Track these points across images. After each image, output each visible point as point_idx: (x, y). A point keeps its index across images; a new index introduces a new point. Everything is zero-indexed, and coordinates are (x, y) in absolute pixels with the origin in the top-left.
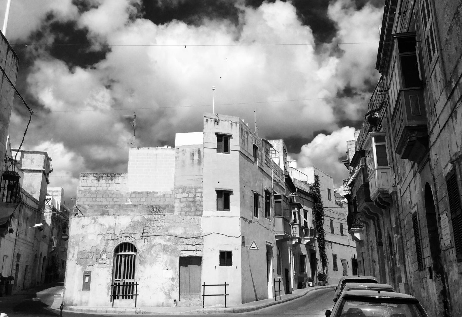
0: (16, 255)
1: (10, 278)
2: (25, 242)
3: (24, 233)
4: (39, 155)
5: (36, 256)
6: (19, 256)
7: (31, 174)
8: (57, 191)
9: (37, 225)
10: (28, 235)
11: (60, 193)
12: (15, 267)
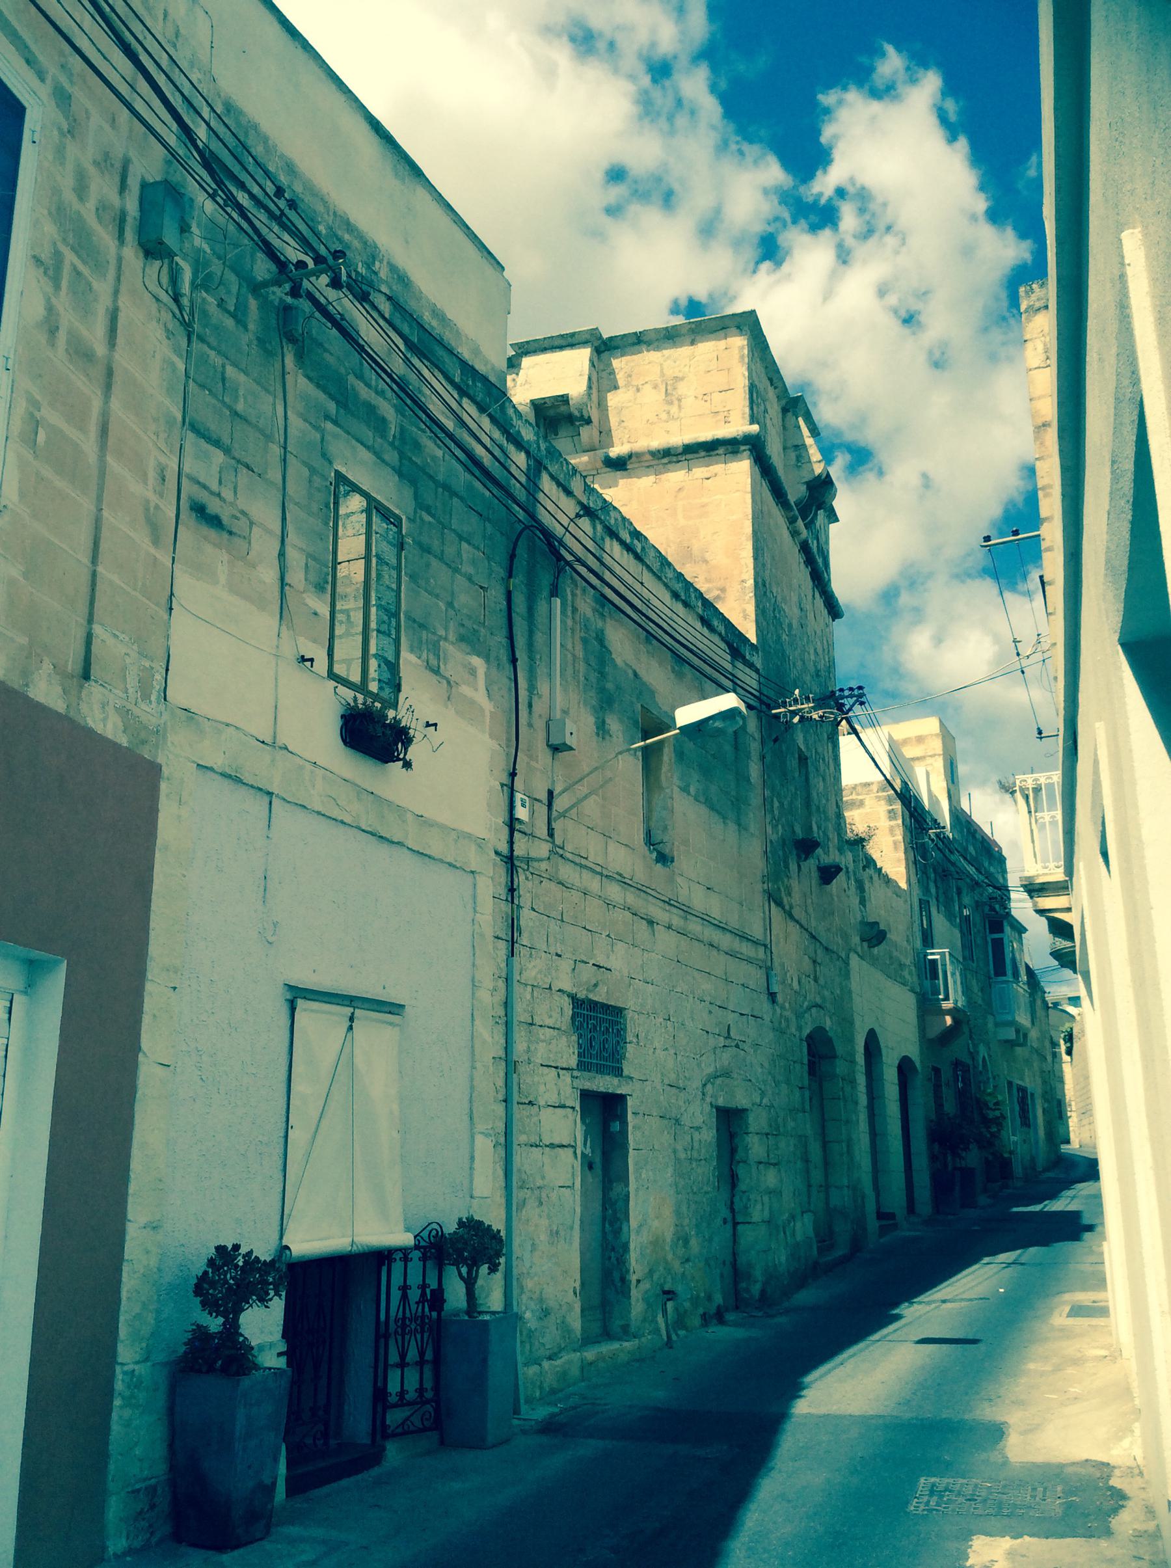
0: (558, 1012)
1: (470, 1246)
2: (657, 912)
4: (707, 349)
5: (819, 1052)
6: (599, 1028)
7: (676, 477)
8: (920, 739)
11: (937, 745)
12: (565, 1126)
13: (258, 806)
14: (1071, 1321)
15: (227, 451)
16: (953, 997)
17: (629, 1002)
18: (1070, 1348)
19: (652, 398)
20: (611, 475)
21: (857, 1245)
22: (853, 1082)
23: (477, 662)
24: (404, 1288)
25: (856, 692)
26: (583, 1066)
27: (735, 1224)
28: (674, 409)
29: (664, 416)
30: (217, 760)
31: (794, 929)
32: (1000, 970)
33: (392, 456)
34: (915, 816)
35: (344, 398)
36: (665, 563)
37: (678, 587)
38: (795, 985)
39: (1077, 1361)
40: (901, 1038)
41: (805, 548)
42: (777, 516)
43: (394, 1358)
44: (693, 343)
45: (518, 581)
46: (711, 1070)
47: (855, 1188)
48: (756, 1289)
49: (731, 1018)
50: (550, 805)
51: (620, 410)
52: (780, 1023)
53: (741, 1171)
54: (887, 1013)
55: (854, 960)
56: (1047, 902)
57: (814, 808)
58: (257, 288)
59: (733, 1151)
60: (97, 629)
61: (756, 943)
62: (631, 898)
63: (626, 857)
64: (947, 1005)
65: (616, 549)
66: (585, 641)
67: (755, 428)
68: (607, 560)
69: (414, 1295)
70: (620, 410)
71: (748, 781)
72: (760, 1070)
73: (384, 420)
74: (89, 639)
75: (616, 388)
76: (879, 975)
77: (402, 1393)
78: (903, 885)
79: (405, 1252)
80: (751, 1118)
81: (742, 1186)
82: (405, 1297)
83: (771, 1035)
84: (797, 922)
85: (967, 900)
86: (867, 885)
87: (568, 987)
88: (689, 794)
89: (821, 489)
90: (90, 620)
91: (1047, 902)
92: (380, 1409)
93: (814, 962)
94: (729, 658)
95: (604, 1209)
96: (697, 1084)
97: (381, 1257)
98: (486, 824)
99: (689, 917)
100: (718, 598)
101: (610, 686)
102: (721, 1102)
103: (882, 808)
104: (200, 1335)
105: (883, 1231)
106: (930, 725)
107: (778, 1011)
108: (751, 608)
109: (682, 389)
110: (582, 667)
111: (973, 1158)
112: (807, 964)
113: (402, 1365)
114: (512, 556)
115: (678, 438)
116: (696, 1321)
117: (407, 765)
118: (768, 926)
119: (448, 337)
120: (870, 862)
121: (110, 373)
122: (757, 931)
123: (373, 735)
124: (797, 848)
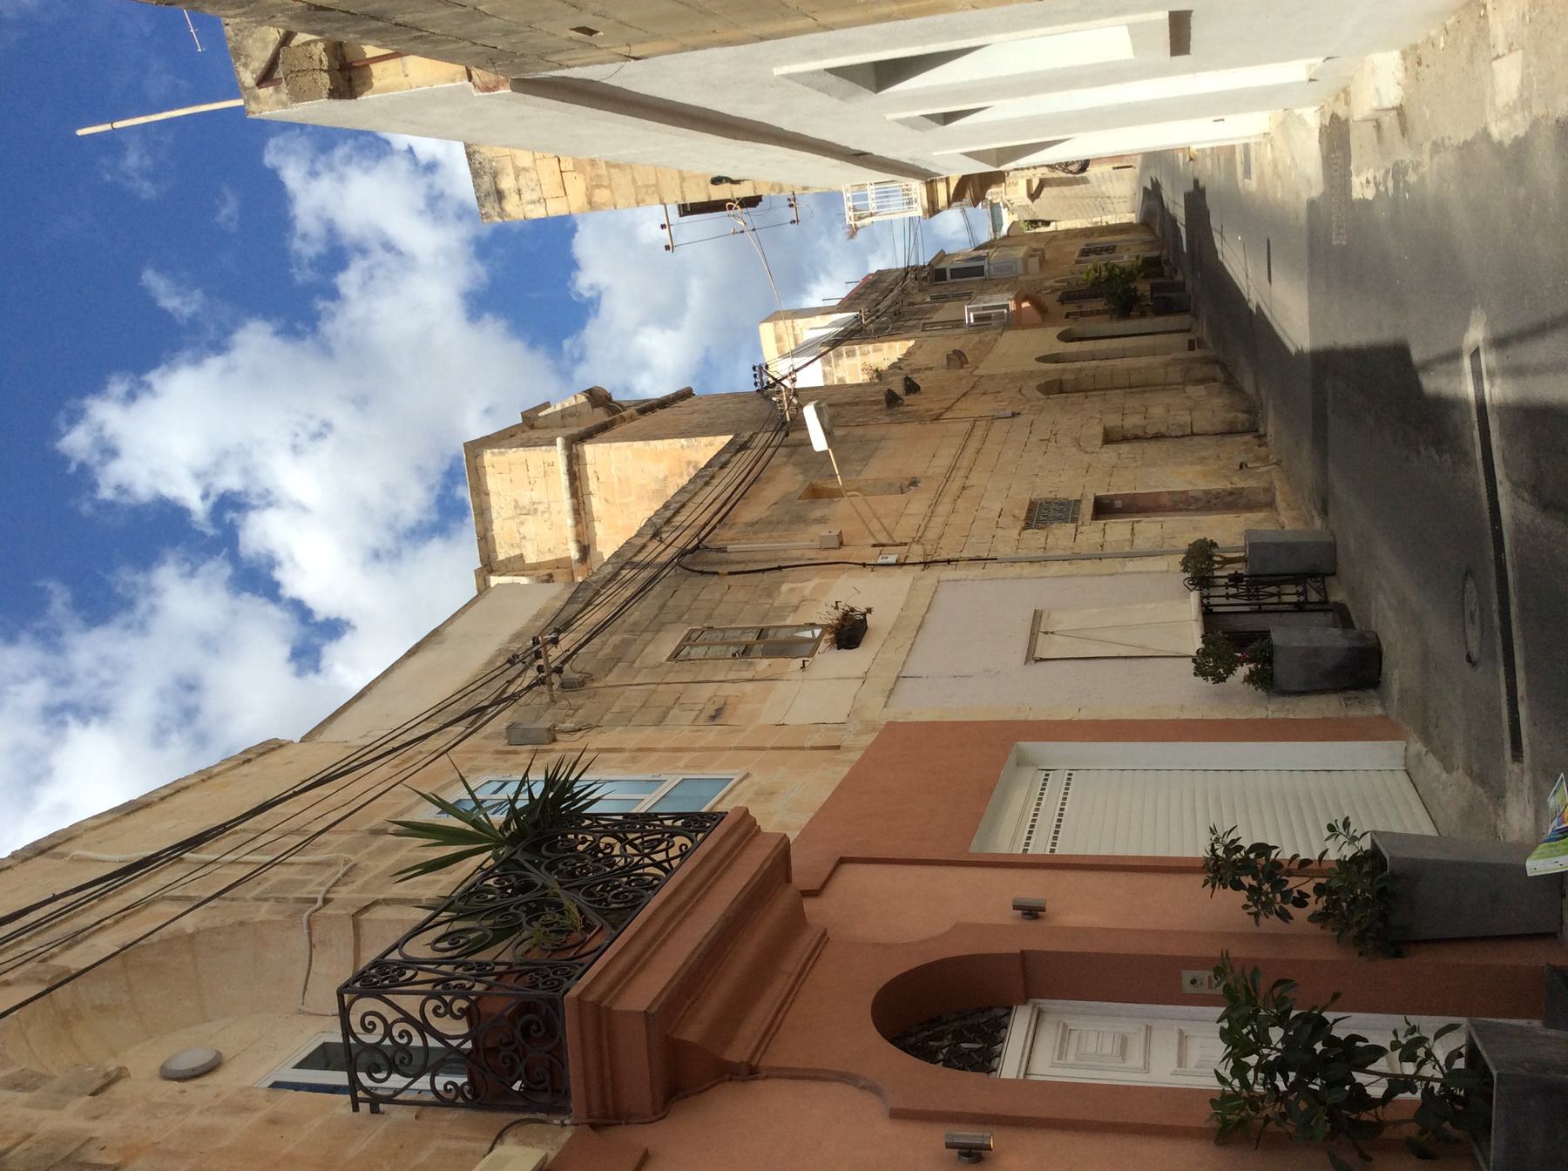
0: (1035, 538)
1: (1200, 565)
2: (955, 485)
3: (896, 501)
4: (492, 482)
5: (1054, 388)
7: (596, 504)
8: (779, 339)
9: (819, 442)
10: (917, 471)
12: (1117, 530)
13: (905, 685)
14: (1254, 176)
15: (670, 708)
16: (1005, 301)
17: (1025, 497)
18: (1269, 171)
19: (531, 527)
20: (593, 558)
21: (1215, 361)
22: (1080, 370)
23: (785, 588)
24: (1227, 596)
26: (1074, 520)
27: (1193, 434)
28: (541, 508)
29: (546, 515)
30: (881, 700)
32: (979, 271)
33: (647, 636)
34: (850, 336)
35: (615, 660)
36: (683, 490)
37: (700, 483)
39: (1275, 164)
40: (1045, 339)
42: (617, 430)
43: (1274, 599)
44: (488, 494)
45: (722, 569)
47: (1166, 365)
48: (1242, 417)
49: (1034, 438)
50: (883, 545)
51: (541, 553)
53: (1152, 430)
54: (1025, 349)
56: (942, 198)
58: (553, 701)
60: (808, 744)
62: (947, 499)
63: (918, 504)
64: (1012, 307)
65: (678, 519)
66: (755, 533)
67: (559, 441)
68: (686, 524)
69: (1232, 591)
70: (541, 553)
73: (623, 641)
74: (813, 748)
75: (521, 556)
77: (1298, 594)
78: (911, 343)
79: (1202, 597)
80: (1109, 424)
81: (1163, 430)
82: (1234, 596)
85: (918, 298)
87: (1015, 533)
89: (598, 398)
90: (802, 748)
91: (942, 198)
92: (1309, 607)
95: (1180, 510)
96: (1086, 458)
97: (1207, 613)
98: (902, 580)
101: (787, 518)
102: (1099, 442)
103: (846, 362)
104: (1250, 679)
106: (767, 331)
108: (704, 440)
109: (525, 501)
110: (775, 534)
111: (1143, 287)
113: (1279, 595)
114: (702, 572)
115: (565, 503)
116: (1263, 449)
117: (869, 610)
119: (554, 611)
120: (893, 366)
121: (640, 750)
122: (966, 426)
123: (849, 632)
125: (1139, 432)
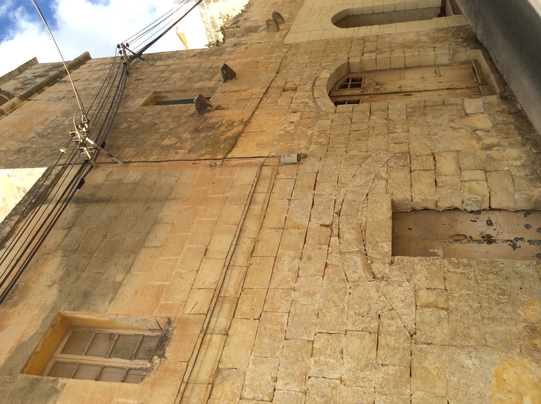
21: (473, 41)
22: (364, 40)
25: (122, 49)
27: (491, 209)
31: (260, 117)
38: (295, 118)
41: (26, 97)
46: (358, 260)
52: (321, 144)
53: (444, 205)
55: (290, 39)
57: (187, 86)
59: (426, 209)
61: (259, 178)
71: (137, 184)
72: (358, 179)
76: (303, 11)
81: (458, 204)
83: (330, 161)
84: (253, 113)
86: (248, 24)
88: (120, 284)
93: (284, 90)
94: (44, 207)
99: (222, 294)
100: (24, 191)
102: (387, 247)
105: (456, 11)
107: (313, 147)
112: (283, 101)
118: (246, 161)
124: (204, 113)
125: (431, 206)
